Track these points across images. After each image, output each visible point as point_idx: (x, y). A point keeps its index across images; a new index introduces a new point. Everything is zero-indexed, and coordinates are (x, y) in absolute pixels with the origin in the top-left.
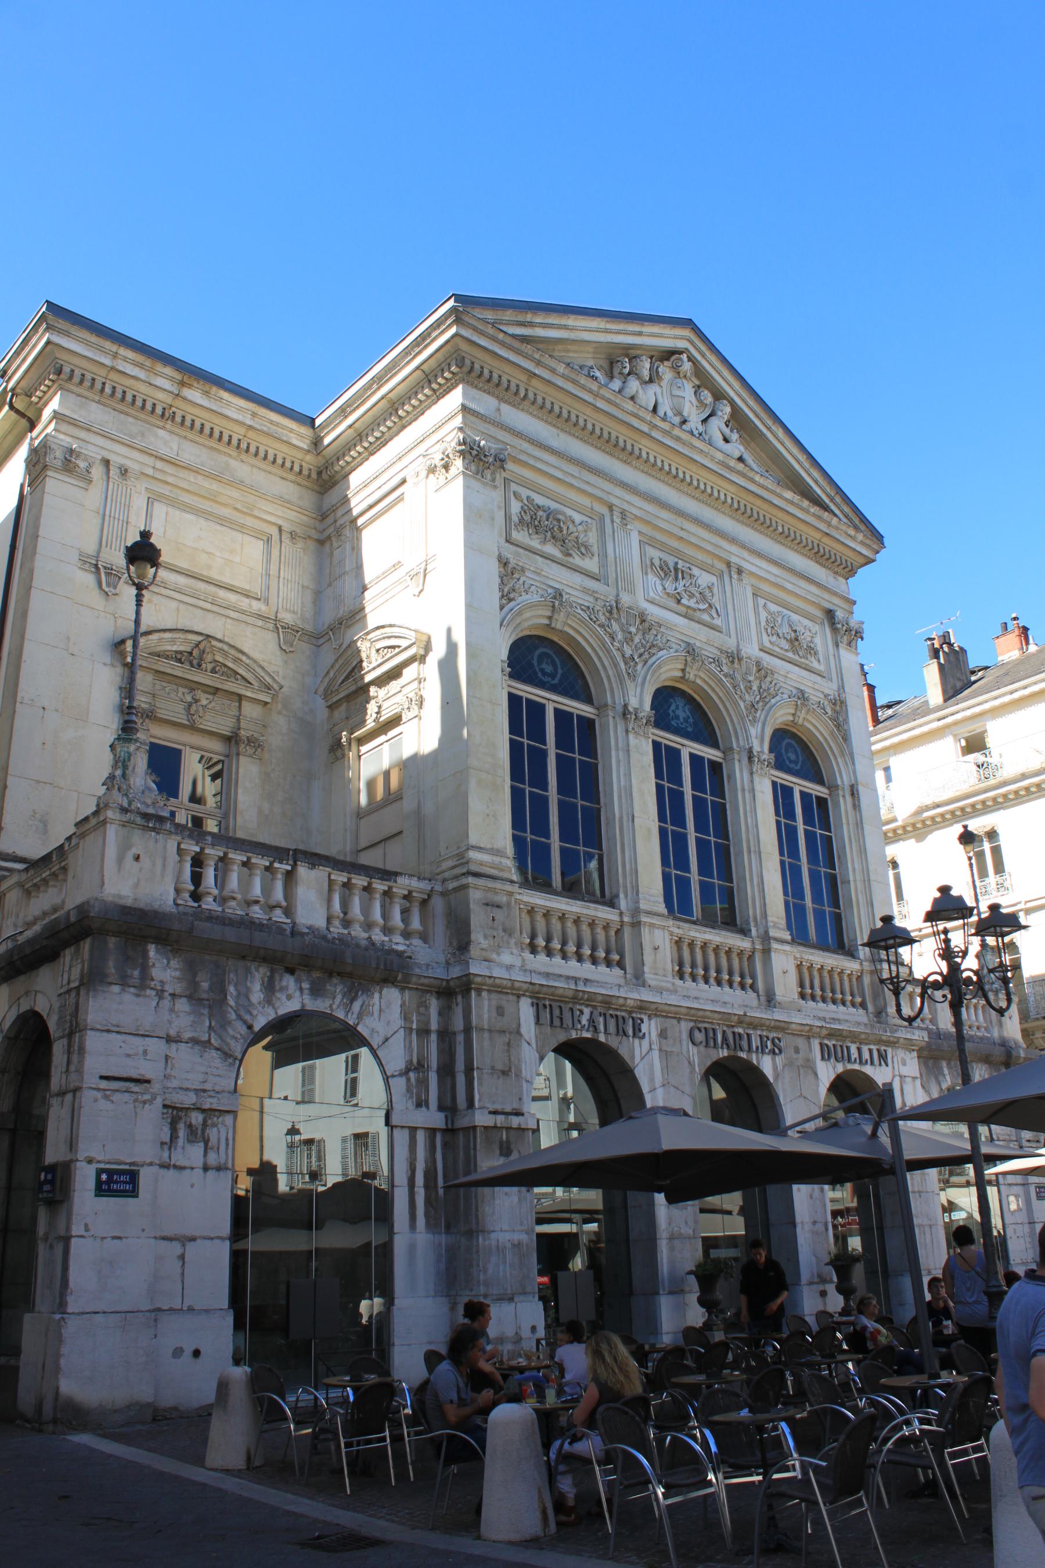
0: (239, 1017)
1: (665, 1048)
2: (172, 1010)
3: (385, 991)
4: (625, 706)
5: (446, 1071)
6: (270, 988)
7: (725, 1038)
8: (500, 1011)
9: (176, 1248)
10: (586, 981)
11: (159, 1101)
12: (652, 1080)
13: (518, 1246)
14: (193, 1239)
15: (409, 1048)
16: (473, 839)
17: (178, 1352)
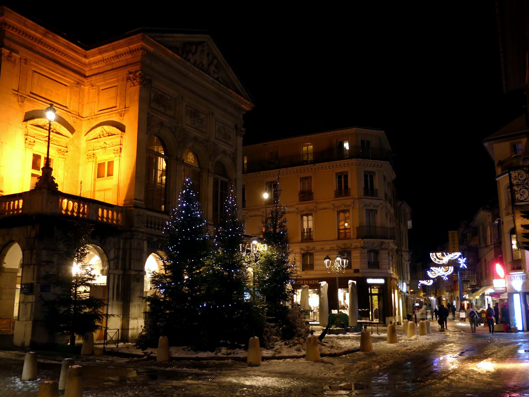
4: (177, 158)
5: (124, 259)
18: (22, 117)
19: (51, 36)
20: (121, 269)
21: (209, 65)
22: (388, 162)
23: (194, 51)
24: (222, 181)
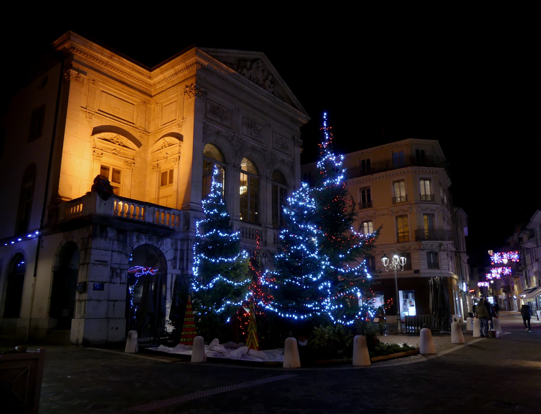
0: (130, 245)
2: (113, 243)
5: (182, 259)
6: (138, 238)
9: (112, 303)
11: (109, 266)
14: (117, 301)
16: (192, 200)
17: (112, 328)
18: (90, 131)
19: (117, 59)
20: (180, 269)
21: (264, 80)
22: (443, 169)
23: (248, 67)
24: (281, 189)
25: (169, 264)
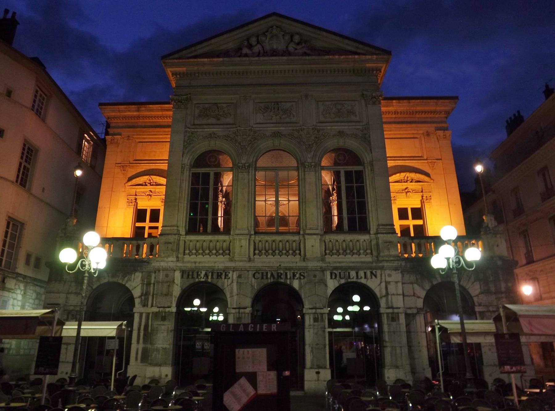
1: (239, 281)
3: (136, 274)
7: (272, 275)
8: (167, 276)
10: (200, 262)
12: (231, 293)
13: (165, 349)
15: (142, 289)
19: (144, 109)
25: (137, 301)
